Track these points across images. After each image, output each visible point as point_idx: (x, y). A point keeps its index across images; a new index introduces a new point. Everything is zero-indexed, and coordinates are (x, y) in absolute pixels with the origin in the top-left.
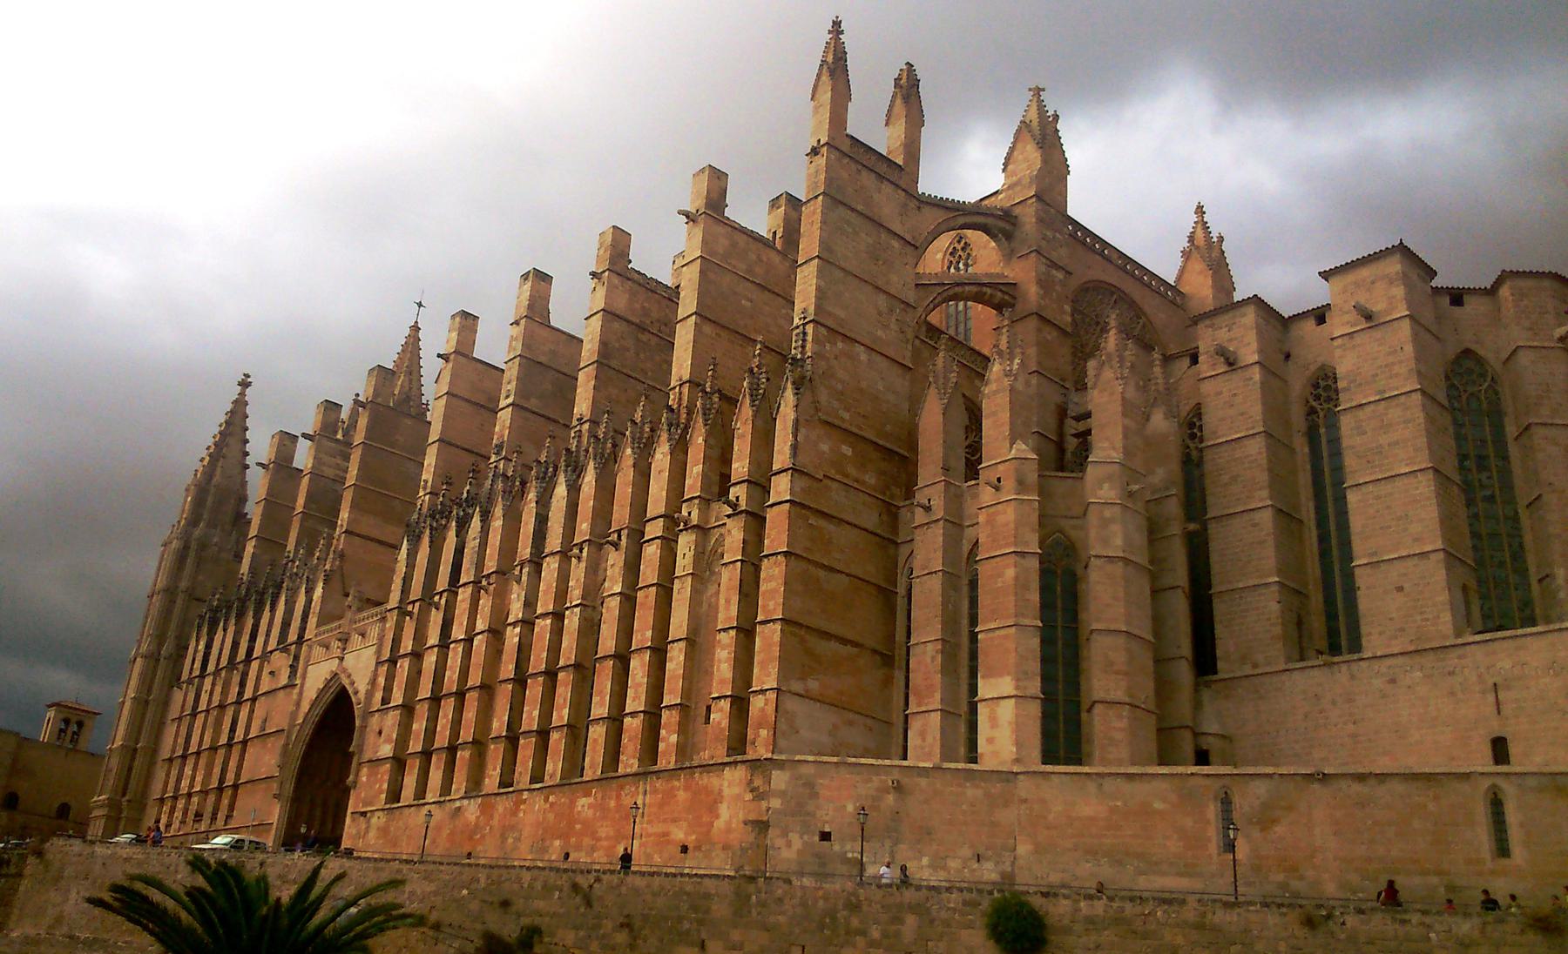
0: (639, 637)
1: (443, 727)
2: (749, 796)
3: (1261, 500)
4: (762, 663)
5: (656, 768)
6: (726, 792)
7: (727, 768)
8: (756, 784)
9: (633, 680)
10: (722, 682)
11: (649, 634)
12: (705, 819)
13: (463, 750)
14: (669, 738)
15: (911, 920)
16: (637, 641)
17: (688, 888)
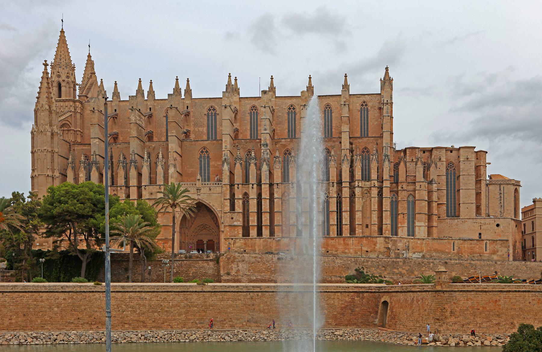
0: (345, 208)
1: (265, 220)
2: (385, 243)
3: (444, 188)
4: (385, 219)
5: (356, 236)
6: (378, 242)
7: (378, 238)
8: (386, 241)
9: (344, 217)
10: (375, 221)
11: (349, 208)
12: (373, 246)
13: (277, 226)
14: (358, 231)
15: (432, 264)
16: (344, 209)
17: (395, 260)
